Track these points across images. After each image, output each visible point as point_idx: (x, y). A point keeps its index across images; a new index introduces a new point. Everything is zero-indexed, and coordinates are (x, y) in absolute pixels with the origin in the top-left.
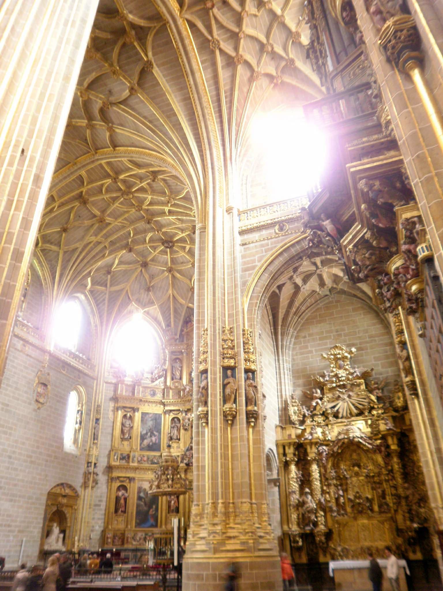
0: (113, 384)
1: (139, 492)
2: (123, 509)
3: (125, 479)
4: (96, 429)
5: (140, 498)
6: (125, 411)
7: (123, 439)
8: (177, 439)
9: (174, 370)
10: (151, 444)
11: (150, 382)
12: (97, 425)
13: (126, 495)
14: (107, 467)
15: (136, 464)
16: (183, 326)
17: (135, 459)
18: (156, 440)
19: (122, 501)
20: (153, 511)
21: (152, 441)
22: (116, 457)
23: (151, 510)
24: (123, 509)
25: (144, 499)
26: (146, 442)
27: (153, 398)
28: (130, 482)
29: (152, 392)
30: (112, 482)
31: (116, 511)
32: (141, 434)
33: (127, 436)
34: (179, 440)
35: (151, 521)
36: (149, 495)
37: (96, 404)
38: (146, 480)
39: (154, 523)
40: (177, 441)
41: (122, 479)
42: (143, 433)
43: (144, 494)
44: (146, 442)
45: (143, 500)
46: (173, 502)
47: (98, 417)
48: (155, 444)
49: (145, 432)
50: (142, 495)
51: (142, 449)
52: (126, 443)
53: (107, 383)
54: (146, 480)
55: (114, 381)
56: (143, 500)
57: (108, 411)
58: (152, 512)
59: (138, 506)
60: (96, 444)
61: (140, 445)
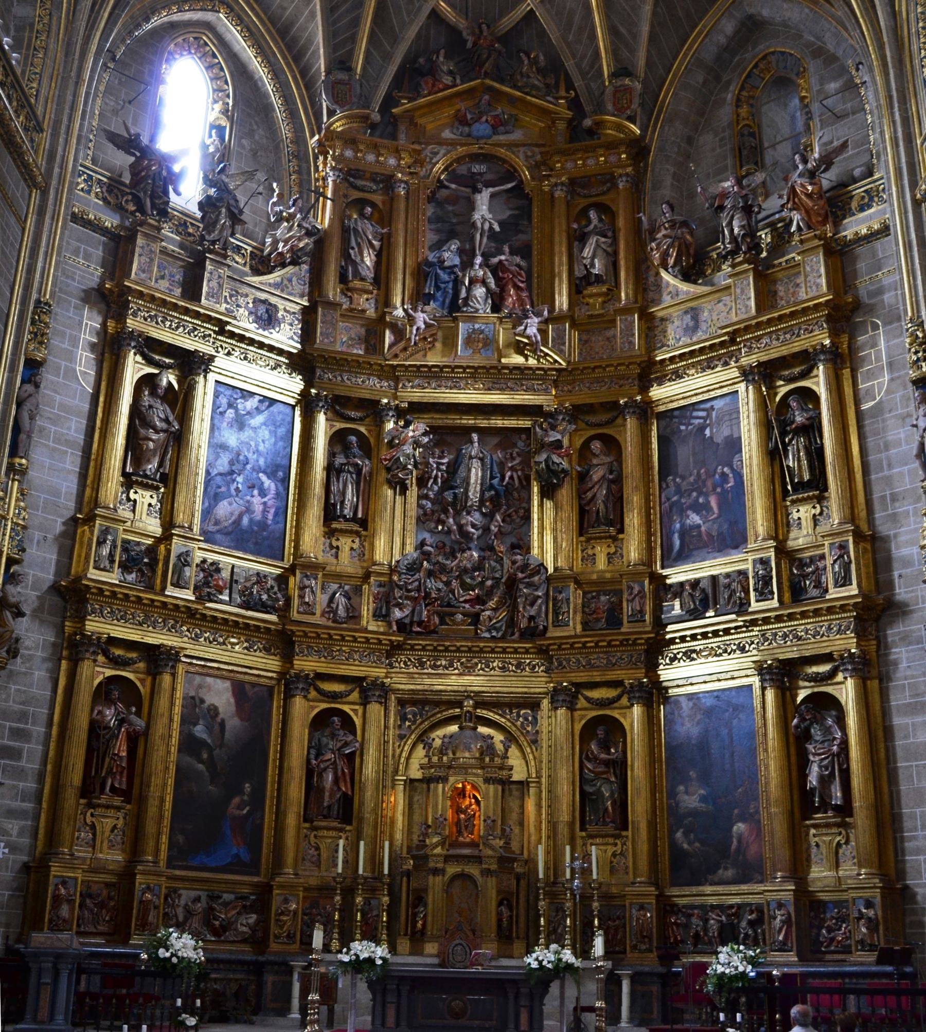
0: (104, 231)
1: (188, 720)
2: (121, 783)
3: (134, 655)
4: (27, 406)
5: (189, 744)
6: (150, 362)
7: (128, 482)
8: (354, 519)
9: (353, 244)
10: (245, 521)
11: (247, 269)
12: (29, 388)
13: (140, 723)
14: (55, 588)
15: (188, 595)
16: (398, 81)
17: (190, 573)
18: (265, 511)
19: (121, 749)
20: (240, 807)
21: (248, 510)
22: (105, 551)
23: (236, 800)
24: (121, 783)
25: (210, 749)
26: (224, 509)
27: (266, 333)
28: (154, 672)
29: (262, 309)
30: (75, 663)
31: (88, 790)
32: (208, 473)
33: (151, 467)
34: (364, 523)
35: (236, 848)
36: (227, 735)
37: (34, 296)
38: (219, 674)
39: (245, 856)
40: (356, 528)
41: (118, 652)
42: (214, 472)
43: (209, 729)
44: (224, 509)
45: (205, 756)
46: (330, 777)
47: (39, 356)
48: (263, 525)
49: (223, 464)
50: (200, 730)
51: (208, 537)
52: (145, 498)
53: (75, 218)
54: (219, 674)
55: (110, 221)
56: (205, 756)
57: (75, 341)
58: (237, 807)
59: (182, 775)
60: (23, 472)
61: (203, 520)
